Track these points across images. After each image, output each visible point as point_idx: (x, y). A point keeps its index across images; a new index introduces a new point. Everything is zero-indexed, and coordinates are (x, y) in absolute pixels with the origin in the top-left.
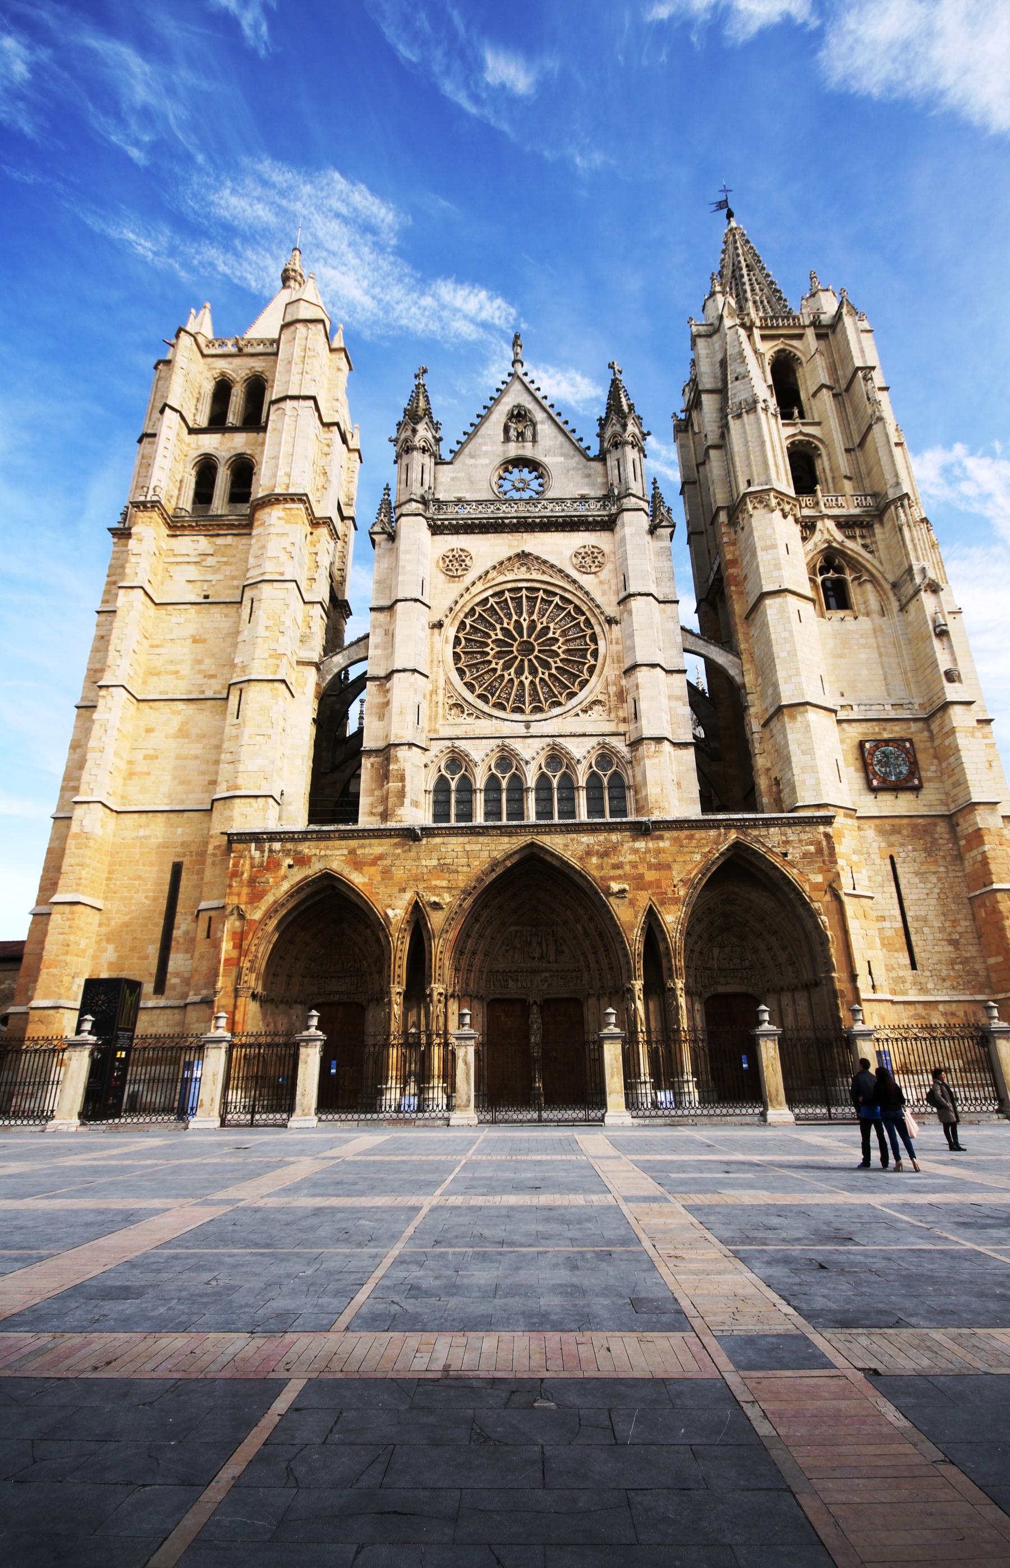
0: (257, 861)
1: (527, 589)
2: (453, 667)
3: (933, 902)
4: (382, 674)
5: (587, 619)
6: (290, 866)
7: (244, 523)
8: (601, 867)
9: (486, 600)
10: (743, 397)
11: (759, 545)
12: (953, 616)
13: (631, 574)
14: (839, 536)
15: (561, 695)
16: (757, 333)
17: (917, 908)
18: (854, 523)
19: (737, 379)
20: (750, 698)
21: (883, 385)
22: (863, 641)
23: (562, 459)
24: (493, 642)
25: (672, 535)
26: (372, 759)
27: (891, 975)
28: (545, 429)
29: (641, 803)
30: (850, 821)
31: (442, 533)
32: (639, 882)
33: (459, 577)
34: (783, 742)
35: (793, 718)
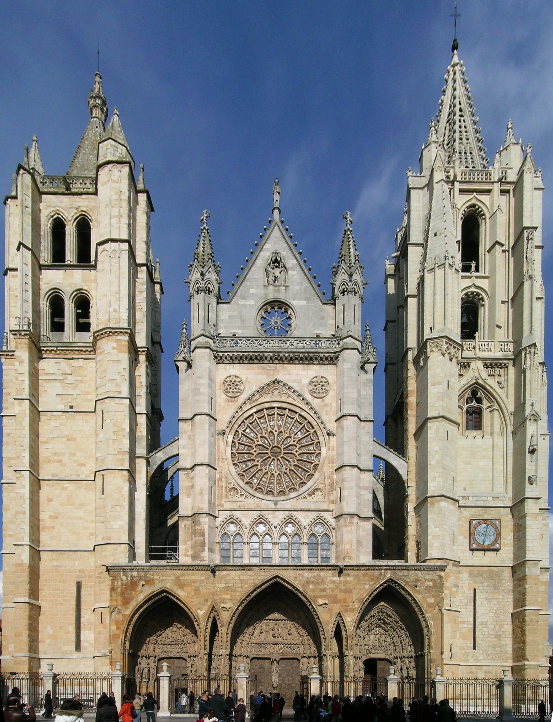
0: (124, 582)
3: (492, 615)
6: (143, 585)
8: (314, 590)
12: (543, 437)
13: (345, 400)
14: (484, 373)
16: (457, 186)
17: (483, 617)
18: (496, 364)
23: (304, 303)
27: (462, 652)
30: (455, 568)
32: (334, 600)
33: (234, 397)
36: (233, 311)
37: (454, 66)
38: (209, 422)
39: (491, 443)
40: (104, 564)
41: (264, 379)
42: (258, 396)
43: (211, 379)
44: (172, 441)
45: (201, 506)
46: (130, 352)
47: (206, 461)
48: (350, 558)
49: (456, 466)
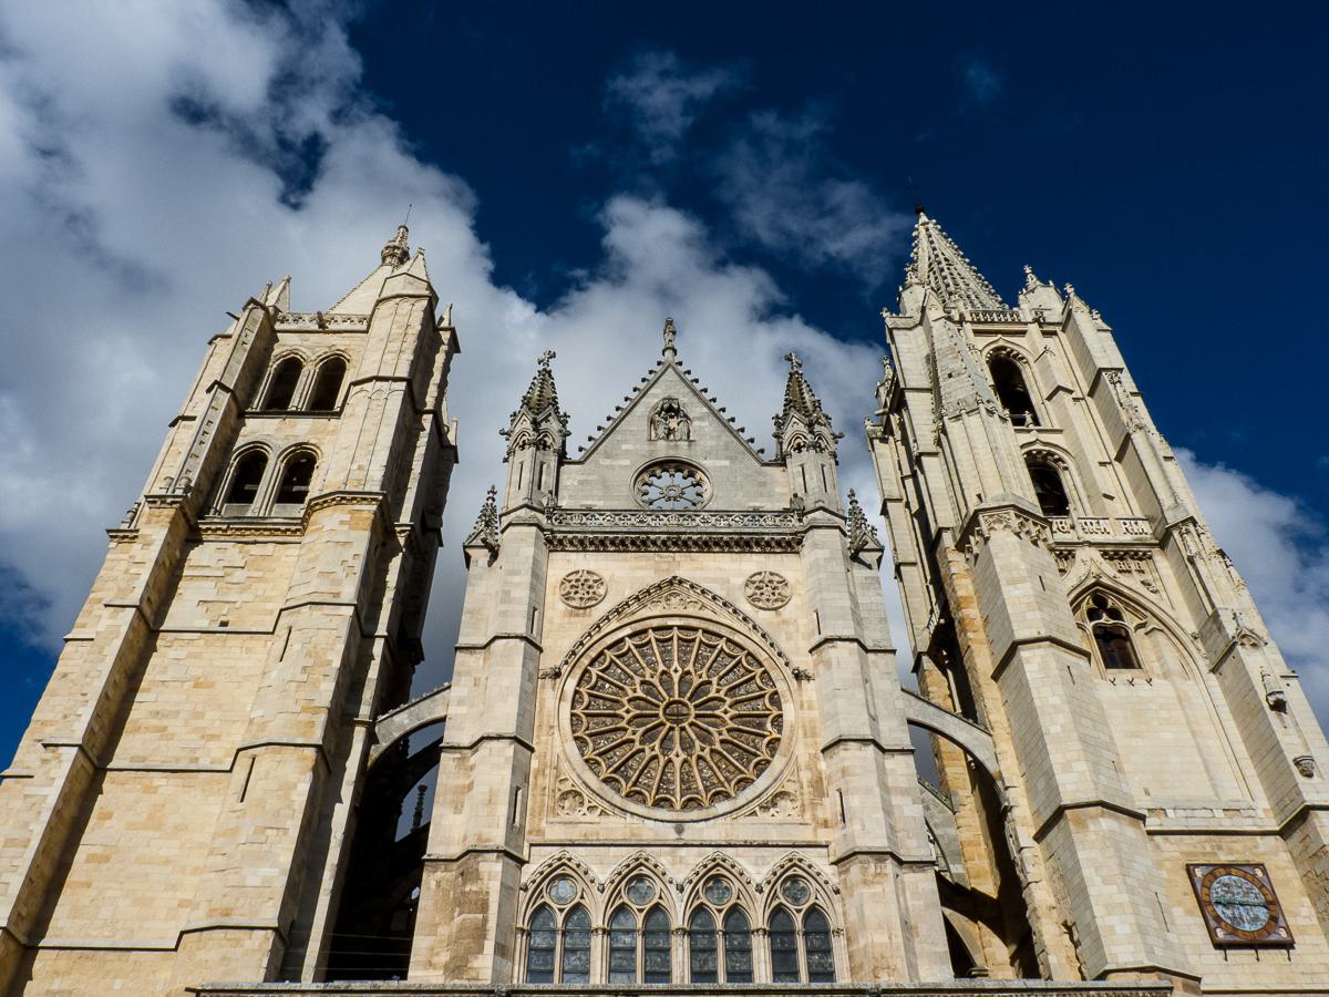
1: (680, 628)
2: (570, 736)
4: (466, 743)
5: (765, 672)
7: (293, 528)
9: (622, 640)
10: (961, 397)
11: (1003, 577)
14: (1109, 569)
15: (729, 782)
16: (968, 327)
18: (1126, 553)
19: (950, 376)
20: (1010, 794)
21: (1136, 391)
22: (1164, 714)
23: (727, 463)
24: (629, 701)
25: (879, 561)
26: (439, 875)
28: (703, 426)
29: (858, 959)
31: (563, 550)
33: (585, 608)
34: (1070, 864)
35: (1082, 824)
36: (589, 474)
37: (923, 224)
38: (525, 650)
39: (1173, 694)
40: (192, 986)
41: (651, 578)
42: (636, 606)
43: (538, 578)
44: (435, 690)
45: (486, 832)
46: (374, 530)
47: (511, 730)
48: (891, 970)
49: (1111, 738)
